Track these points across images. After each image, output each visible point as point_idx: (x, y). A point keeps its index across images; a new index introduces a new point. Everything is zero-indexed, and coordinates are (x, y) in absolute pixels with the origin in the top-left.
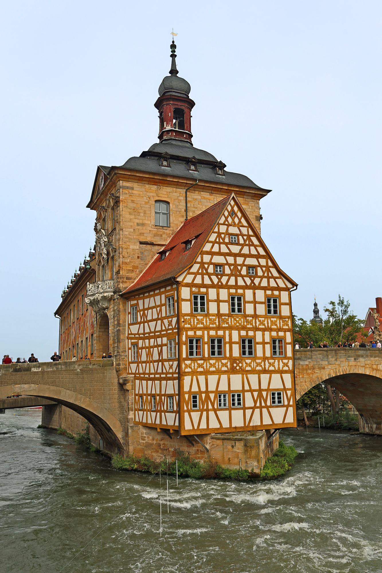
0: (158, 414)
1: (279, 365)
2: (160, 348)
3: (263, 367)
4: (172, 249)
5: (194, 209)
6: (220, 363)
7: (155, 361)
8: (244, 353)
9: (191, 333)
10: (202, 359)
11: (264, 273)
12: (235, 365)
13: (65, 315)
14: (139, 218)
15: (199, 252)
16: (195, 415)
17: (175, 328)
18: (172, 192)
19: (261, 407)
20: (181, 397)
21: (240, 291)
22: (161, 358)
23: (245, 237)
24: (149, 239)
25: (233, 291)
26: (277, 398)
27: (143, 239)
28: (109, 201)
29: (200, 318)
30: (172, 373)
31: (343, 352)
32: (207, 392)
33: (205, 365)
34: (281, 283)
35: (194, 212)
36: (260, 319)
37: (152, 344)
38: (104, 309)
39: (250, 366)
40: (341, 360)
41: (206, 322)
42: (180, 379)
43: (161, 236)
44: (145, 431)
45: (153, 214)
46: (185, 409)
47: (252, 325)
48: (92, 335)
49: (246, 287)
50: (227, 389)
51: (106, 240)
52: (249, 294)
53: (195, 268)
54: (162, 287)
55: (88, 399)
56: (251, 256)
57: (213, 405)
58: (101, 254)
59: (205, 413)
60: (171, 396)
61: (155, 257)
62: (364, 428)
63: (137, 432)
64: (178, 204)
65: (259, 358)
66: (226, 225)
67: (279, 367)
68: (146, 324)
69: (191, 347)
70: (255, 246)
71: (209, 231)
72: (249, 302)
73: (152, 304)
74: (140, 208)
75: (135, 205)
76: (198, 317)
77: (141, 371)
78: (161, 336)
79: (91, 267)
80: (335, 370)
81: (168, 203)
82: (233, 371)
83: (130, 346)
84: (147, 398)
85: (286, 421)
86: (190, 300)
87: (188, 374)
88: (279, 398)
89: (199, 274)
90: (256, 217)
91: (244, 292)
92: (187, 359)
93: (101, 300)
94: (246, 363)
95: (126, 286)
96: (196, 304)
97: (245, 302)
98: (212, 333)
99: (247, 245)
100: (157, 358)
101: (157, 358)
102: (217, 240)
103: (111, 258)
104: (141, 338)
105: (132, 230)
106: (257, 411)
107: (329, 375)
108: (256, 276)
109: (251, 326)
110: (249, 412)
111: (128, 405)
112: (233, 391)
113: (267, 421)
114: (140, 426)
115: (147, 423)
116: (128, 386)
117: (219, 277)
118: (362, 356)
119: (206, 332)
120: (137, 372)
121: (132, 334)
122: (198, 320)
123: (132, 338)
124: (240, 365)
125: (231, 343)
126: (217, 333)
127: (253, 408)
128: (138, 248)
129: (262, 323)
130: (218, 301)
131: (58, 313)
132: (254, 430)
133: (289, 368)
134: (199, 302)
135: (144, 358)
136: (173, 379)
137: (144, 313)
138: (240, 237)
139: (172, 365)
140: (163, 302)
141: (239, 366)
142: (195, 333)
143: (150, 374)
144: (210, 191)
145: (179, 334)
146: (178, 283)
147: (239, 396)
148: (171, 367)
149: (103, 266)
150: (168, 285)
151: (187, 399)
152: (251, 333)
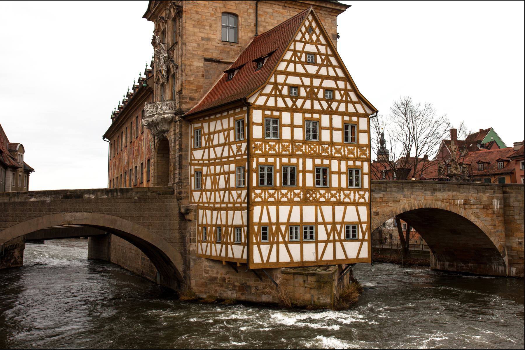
0: (224, 246)
1: (355, 196)
2: (227, 176)
3: (338, 198)
4: (240, 67)
5: (264, 24)
6: (292, 193)
7: (221, 190)
8: (318, 183)
9: (262, 160)
11: (342, 96)
12: (308, 195)
13: (116, 138)
14: (204, 31)
15: (273, 71)
16: (265, 248)
17: (244, 154)
18: (241, 4)
19: (334, 241)
20: (250, 228)
21: (316, 116)
22: (228, 187)
23: (323, 57)
24: (215, 55)
25: (308, 115)
26: (351, 231)
27: (208, 55)
28: (170, 11)
30: (241, 203)
31: (419, 185)
32: (278, 224)
33: (276, 195)
34: (360, 109)
35: (265, 27)
36: (336, 147)
38: (164, 132)
39: (324, 197)
40: (417, 193)
41: (279, 148)
43: (228, 52)
44: (208, 264)
45: (220, 27)
46: (254, 241)
47: (328, 153)
48: (149, 160)
49: (322, 112)
50: (299, 221)
51: (166, 55)
52: (325, 120)
53: (268, 89)
55: (146, 229)
56: (328, 77)
58: (160, 71)
59: (275, 246)
60: (238, 228)
61: (221, 76)
62: (436, 265)
63: (200, 265)
64: (247, 17)
65: (334, 189)
66: (303, 42)
67: (355, 199)
68: (212, 150)
71: (285, 48)
72: (325, 128)
73: (219, 128)
74: (205, 21)
75: (199, 17)
76: (270, 143)
77: (205, 200)
78: (229, 163)
79: (148, 85)
80: (410, 204)
81: (236, 16)
82: (305, 201)
83: (193, 173)
84: (211, 229)
85: (361, 256)
86: (261, 124)
87: (258, 204)
88: (354, 232)
89: (272, 96)
90: (333, 35)
91: (320, 117)
92: (257, 188)
93: (160, 122)
94: (320, 194)
96: (268, 129)
97: (321, 128)
98: (285, 160)
99: (324, 66)
102: (293, 59)
103: (171, 76)
104: (205, 165)
105: (196, 45)
106: (330, 245)
107: (404, 208)
108: (334, 100)
109: (327, 154)
110: (321, 246)
111: (190, 236)
112: (305, 223)
113: (340, 256)
114: (204, 260)
115: (211, 255)
116: (191, 216)
117: (294, 99)
118: (440, 190)
119: (278, 159)
120: (201, 201)
121: (195, 160)
122: (270, 146)
123: (195, 165)
124: (314, 195)
125: (304, 172)
126: (289, 161)
127: (326, 242)
128: (202, 65)
129: (338, 151)
130: (292, 126)
131: (108, 135)
132: (327, 265)
133: (365, 200)
134: (272, 126)
135: (208, 185)
136: (241, 209)
137: (209, 138)
138: (318, 57)
139: (241, 194)
140: (232, 125)
141: (313, 197)
142: (266, 160)
143: (215, 203)
144: (283, 4)
146: (249, 105)
147: (311, 228)
148: (239, 196)
149: (162, 85)
151: (256, 231)
152: (326, 162)
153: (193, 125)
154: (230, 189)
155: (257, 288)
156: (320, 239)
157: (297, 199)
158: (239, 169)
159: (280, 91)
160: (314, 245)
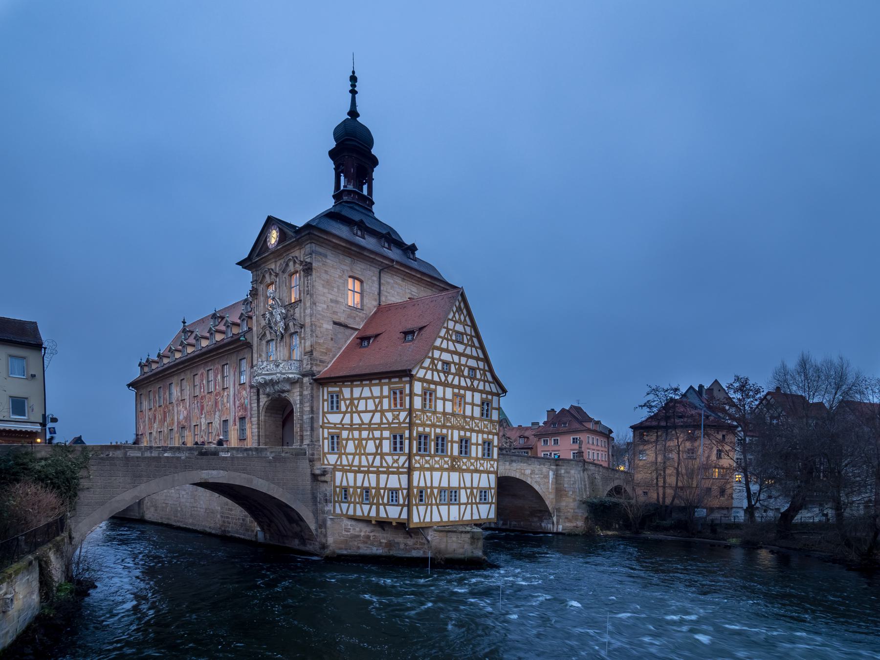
2: (377, 442)
4: (377, 336)
9: (421, 429)
19: (472, 504)
43: (355, 318)
54: (385, 378)
69: (420, 443)
83: (326, 435)
92: (417, 455)
95: (323, 371)
96: (425, 399)
100: (374, 451)
101: (374, 451)
104: (346, 429)
123: (329, 428)
137: (352, 403)
140: (386, 392)
145: (410, 429)
146: (412, 377)
150: (395, 377)
153: (325, 389)
154: (382, 455)
157: (446, 466)
158: (395, 437)
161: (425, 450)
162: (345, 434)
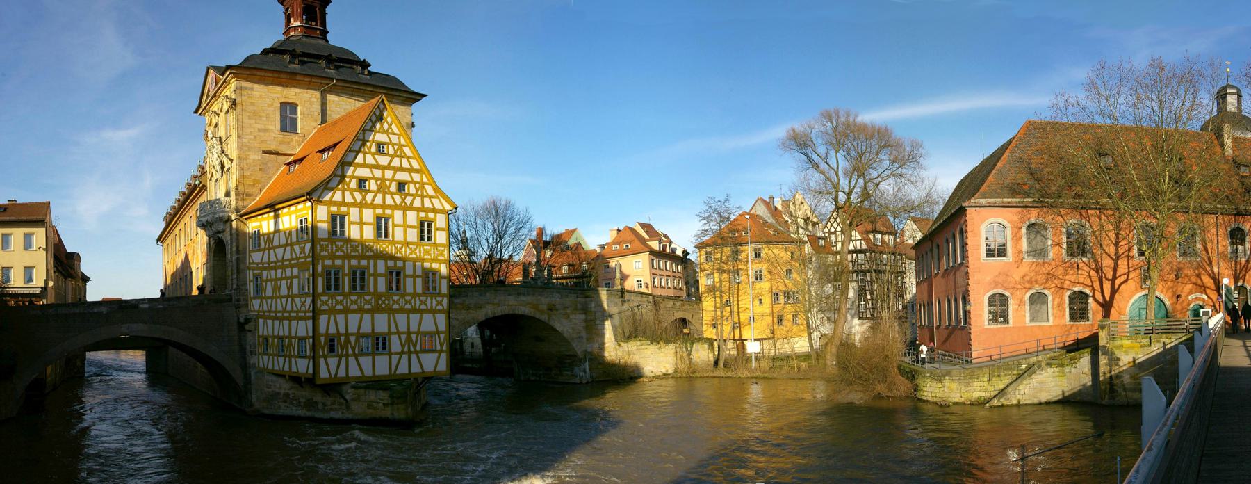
9: (328, 262)
10: (343, 294)
16: (333, 361)
19: (409, 353)
21: (388, 212)
25: (379, 211)
29: (339, 243)
30: (305, 312)
32: (347, 335)
37: (279, 276)
42: (315, 319)
49: (395, 207)
52: (398, 215)
56: (402, 169)
57: (353, 349)
60: (302, 339)
65: (409, 295)
70: (408, 158)
72: (398, 226)
78: (292, 266)
82: (377, 309)
85: (438, 369)
87: (324, 312)
92: (324, 293)
97: (395, 226)
98: (354, 262)
104: (265, 269)
106: (405, 357)
110: (395, 358)
113: (416, 369)
123: (254, 269)
125: (376, 275)
132: (401, 380)
135: (269, 292)
136: (305, 318)
143: (276, 312)
148: (303, 304)
154: (293, 296)
155: (324, 405)
156: (393, 350)
157: (368, 306)
159: (348, 185)
160: (387, 357)
161: (337, 287)
162: (265, 273)
